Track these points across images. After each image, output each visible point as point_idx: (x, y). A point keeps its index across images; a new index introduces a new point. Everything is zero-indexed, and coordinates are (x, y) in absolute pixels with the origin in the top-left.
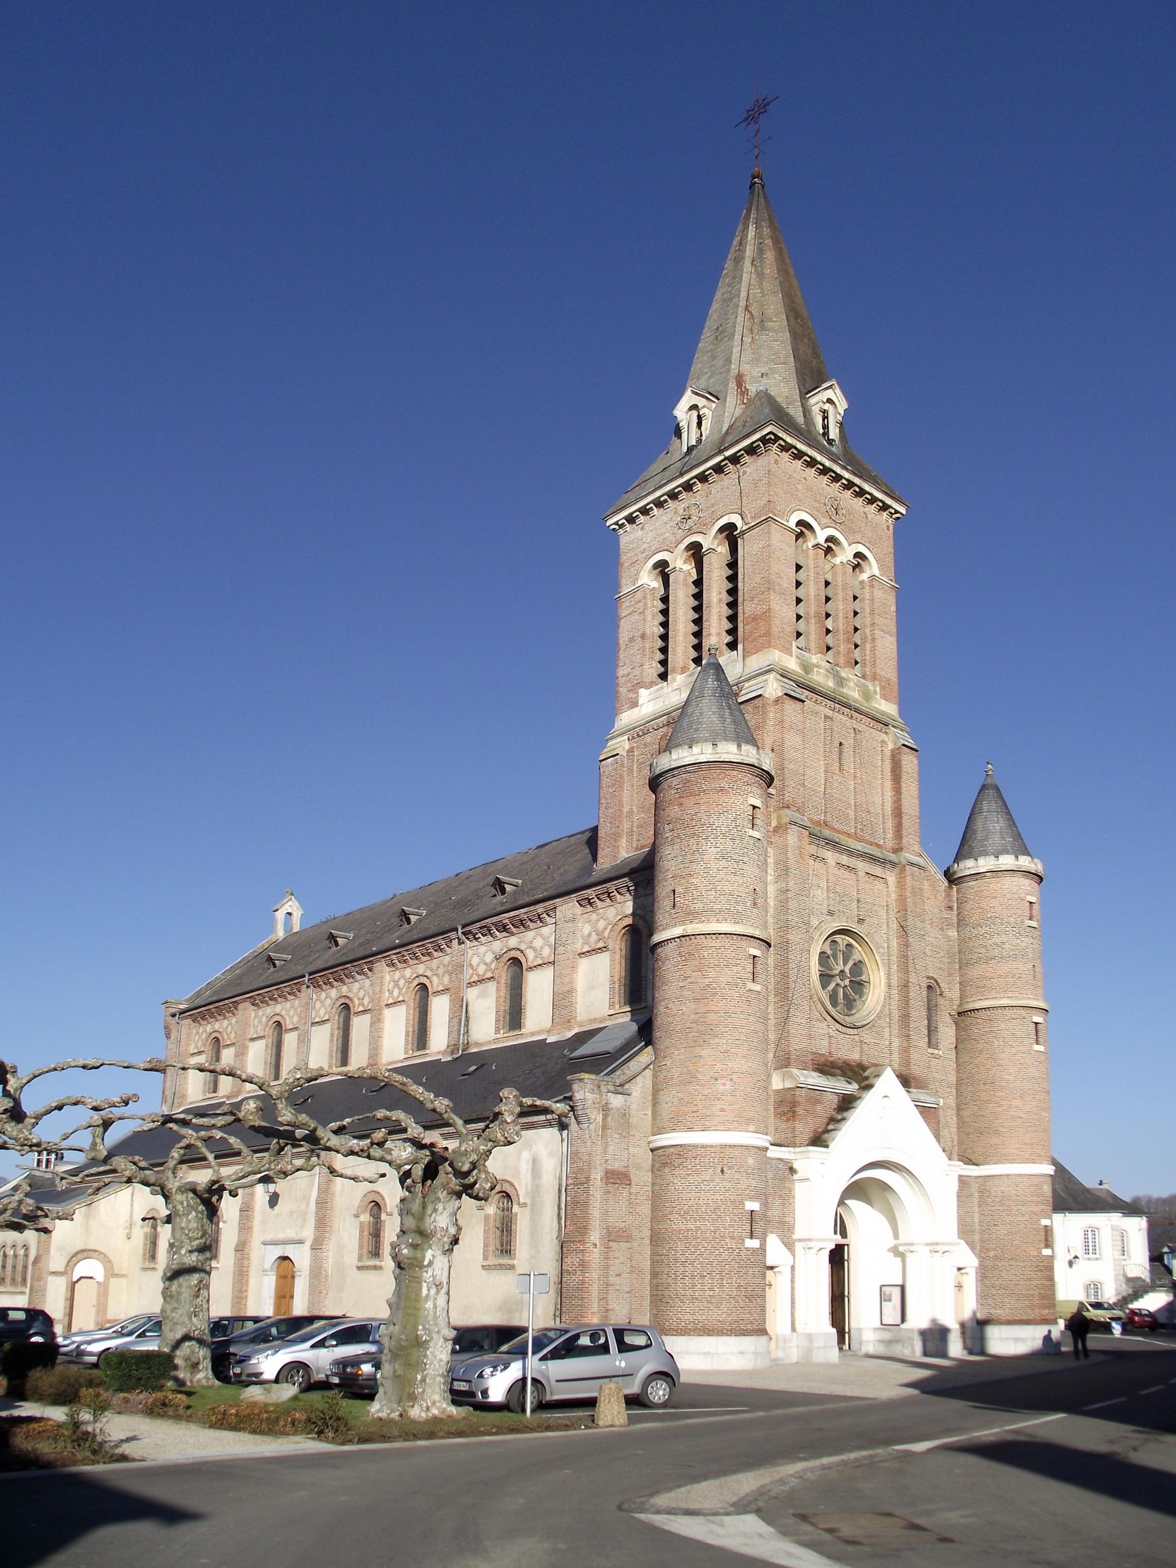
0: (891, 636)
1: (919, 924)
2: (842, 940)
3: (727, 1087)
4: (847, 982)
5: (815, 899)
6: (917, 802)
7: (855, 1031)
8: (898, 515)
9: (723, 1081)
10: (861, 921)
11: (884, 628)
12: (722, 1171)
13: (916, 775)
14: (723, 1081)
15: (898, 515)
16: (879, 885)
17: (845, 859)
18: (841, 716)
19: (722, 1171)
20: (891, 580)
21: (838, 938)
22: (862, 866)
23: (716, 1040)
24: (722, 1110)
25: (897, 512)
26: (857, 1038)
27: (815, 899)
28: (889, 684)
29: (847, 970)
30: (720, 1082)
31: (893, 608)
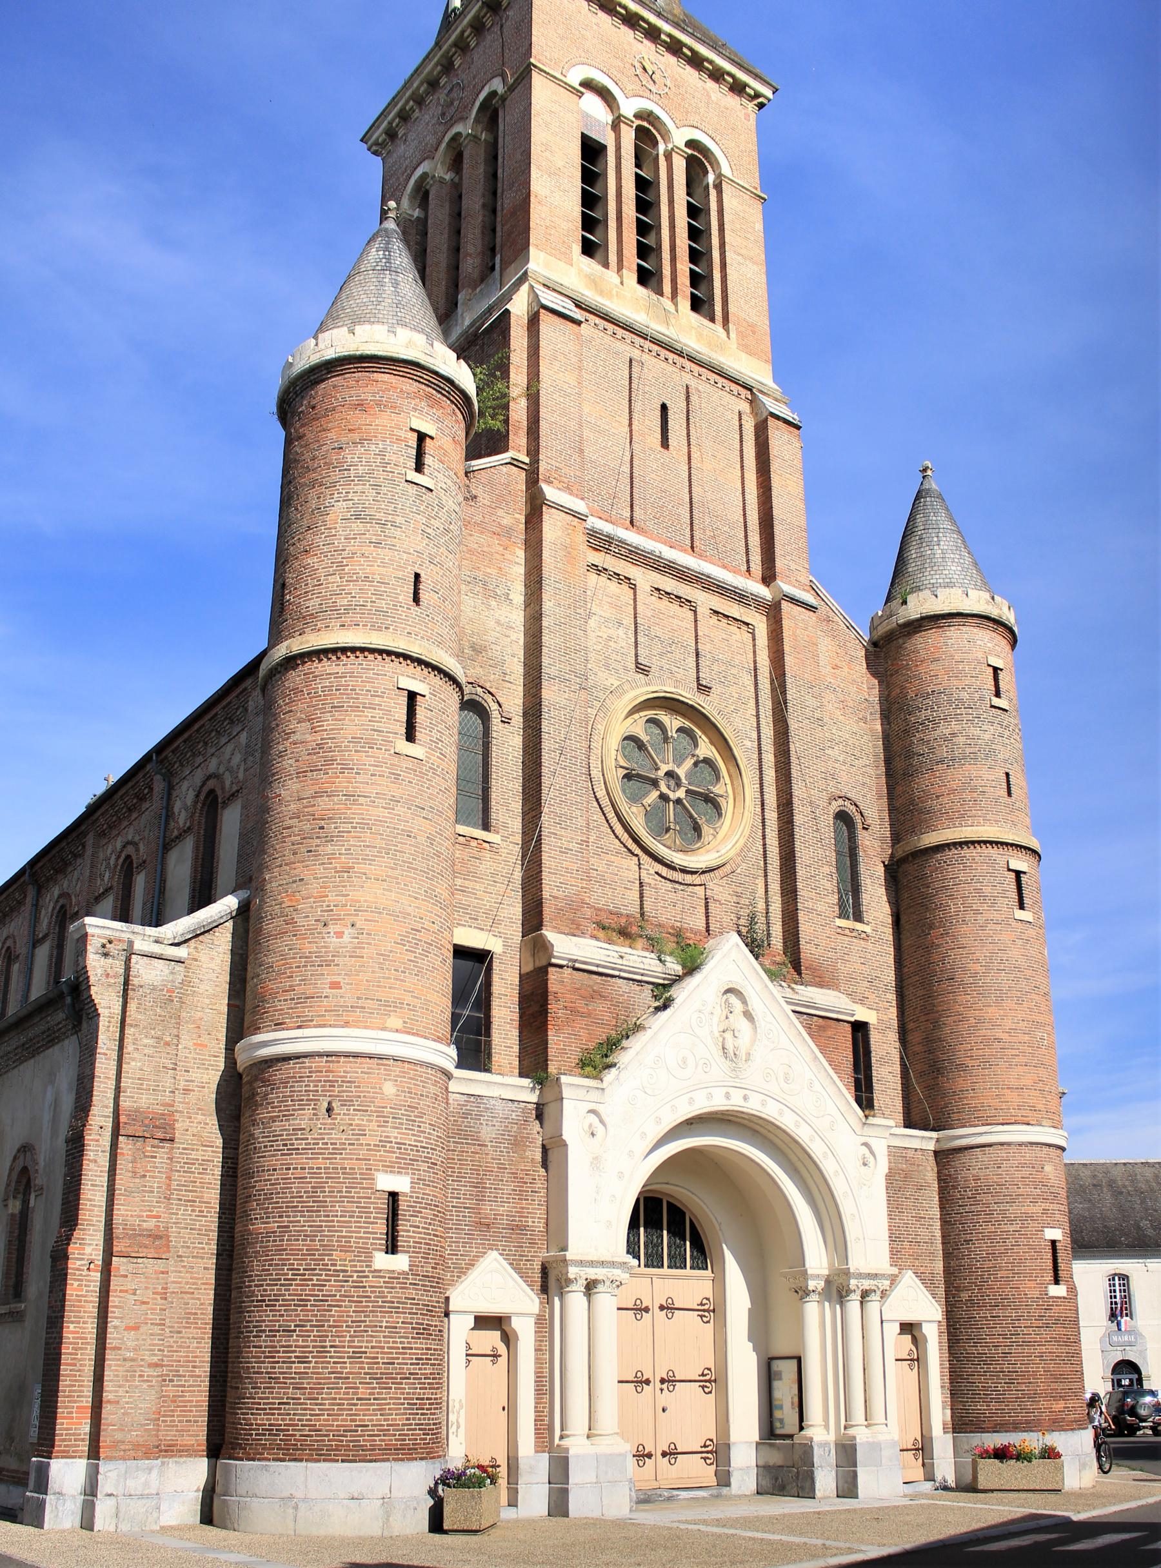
0: (756, 263)
1: (811, 702)
2: (672, 723)
3: (346, 938)
4: (681, 793)
5: (612, 644)
6: (802, 506)
7: (696, 879)
8: (761, 100)
9: (338, 928)
10: (703, 688)
11: (743, 251)
12: (329, 1110)
13: (798, 463)
14: (338, 928)
15: (761, 100)
16: (744, 635)
17: (669, 584)
18: (664, 365)
19: (329, 1110)
20: (756, 189)
21: (665, 718)
22: (705, 600)
23: (329, 849)
24: (335, 985)
25: (757, 95)
26: (700, 891)
27: (612, 644)
28: (754, 332)
29: (681, 772)
30: (332, 928)
31: (759, 226)
